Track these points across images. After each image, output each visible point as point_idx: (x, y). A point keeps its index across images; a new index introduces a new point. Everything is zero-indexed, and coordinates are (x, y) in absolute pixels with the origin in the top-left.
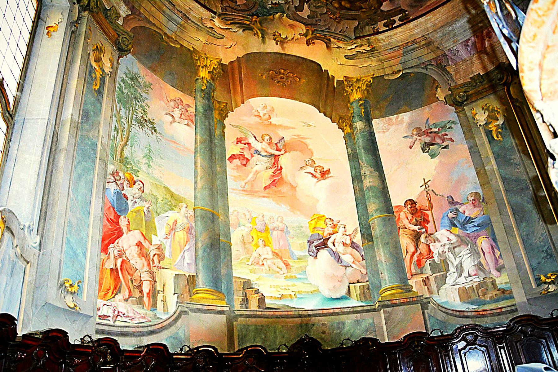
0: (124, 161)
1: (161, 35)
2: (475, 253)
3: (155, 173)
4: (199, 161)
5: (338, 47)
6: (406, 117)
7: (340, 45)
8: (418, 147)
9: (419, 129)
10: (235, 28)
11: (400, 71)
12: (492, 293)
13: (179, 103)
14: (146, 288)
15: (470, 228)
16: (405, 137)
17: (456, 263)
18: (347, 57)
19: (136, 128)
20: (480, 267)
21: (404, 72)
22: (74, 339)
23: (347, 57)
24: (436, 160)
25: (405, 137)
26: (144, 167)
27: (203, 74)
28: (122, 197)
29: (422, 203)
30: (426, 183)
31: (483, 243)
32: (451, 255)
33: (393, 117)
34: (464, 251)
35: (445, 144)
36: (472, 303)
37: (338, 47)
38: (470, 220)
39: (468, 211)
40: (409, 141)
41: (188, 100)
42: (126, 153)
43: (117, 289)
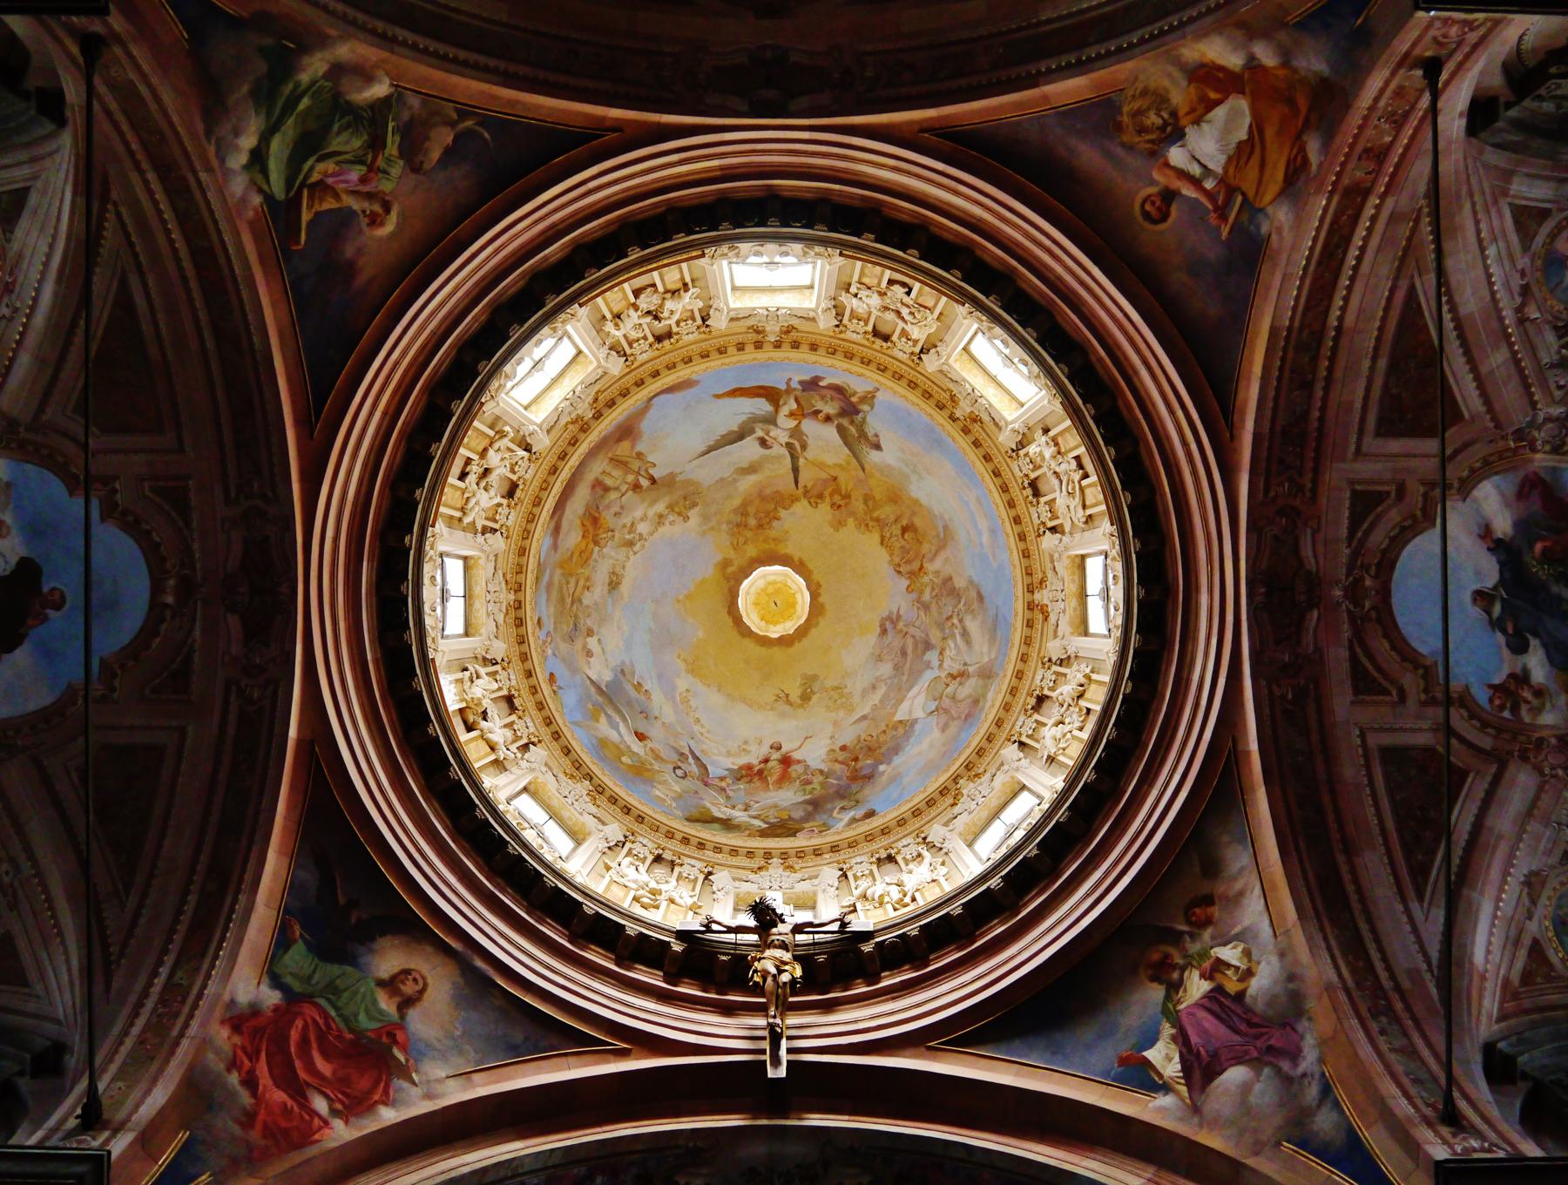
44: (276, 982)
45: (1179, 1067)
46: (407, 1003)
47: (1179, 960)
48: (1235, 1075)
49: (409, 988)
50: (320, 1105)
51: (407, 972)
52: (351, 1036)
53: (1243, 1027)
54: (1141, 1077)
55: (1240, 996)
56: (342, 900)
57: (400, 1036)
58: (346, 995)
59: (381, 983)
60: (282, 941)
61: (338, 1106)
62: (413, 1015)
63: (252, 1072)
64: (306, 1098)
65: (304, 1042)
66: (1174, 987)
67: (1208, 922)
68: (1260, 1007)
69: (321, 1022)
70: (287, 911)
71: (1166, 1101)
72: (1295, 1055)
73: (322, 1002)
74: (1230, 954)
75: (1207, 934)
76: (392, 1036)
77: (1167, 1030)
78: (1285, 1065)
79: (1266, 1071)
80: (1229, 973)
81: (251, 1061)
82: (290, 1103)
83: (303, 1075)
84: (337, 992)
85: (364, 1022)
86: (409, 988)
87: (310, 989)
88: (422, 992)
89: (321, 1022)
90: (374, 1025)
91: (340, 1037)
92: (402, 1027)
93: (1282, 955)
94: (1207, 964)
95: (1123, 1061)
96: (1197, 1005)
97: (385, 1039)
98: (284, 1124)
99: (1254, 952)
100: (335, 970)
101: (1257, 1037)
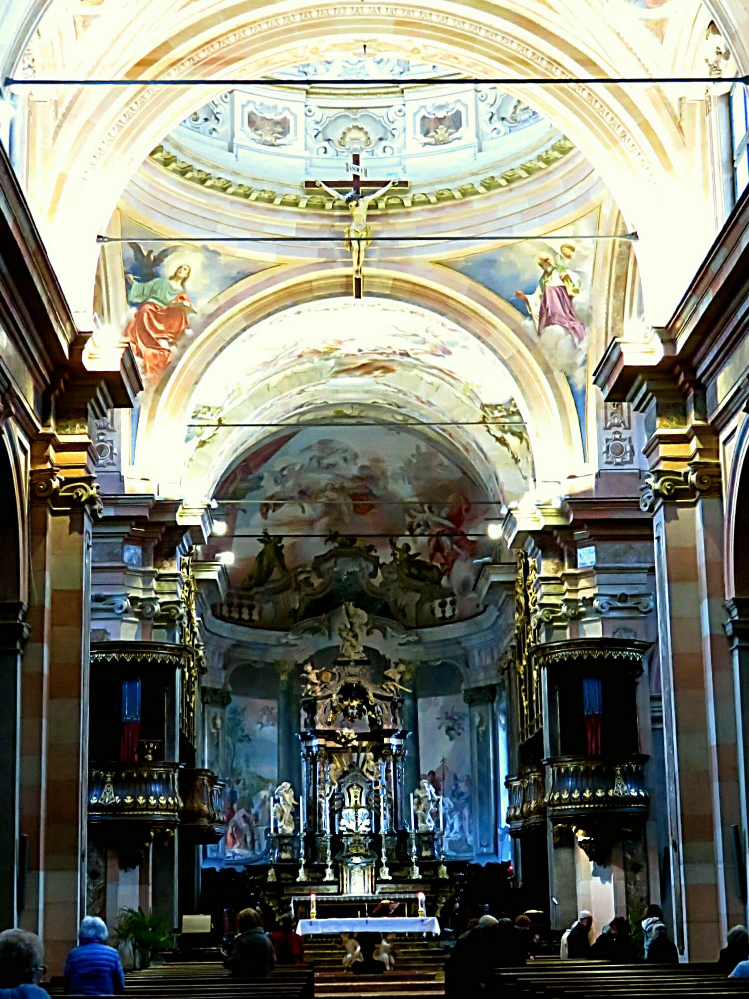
0: (233, 770)
1: (249, 665)
2: (461, 818)
3: (252, 769)
4: (281, 748)
5: (393, 636)
6: (441, 700)
7: (394, 634)
8: (443, 729)
9: (446, 713)
10: (306, 635)
11: (438, 660)
12: (464, 847)
13: (267, 710)
14: (249, 839)
15: (462, 801)
16: (438, 718)
17: (451, 822)
18: (400, 645)
19: (239, 745)
20: (461, 828)
21: (445, 661)
22: (218, 870)
23: (400, 645)
24: (452, 743)
25: (438, 718)
26: (244, 769)
27: (283, 677)
28: (233, 793)
29: (439, 775)
30: (443, 760)
31: (466, 812)
32: (449, 817)
33: (433, 698)
34: (456, 816)
35: (460, 731)
36: (454, 851)
37: (393, 636)
38: (462, 794)
39: (463, 787)
40: (439, 722)
41: (273, 704)
42: (234, 765)
43: (234, 843)
44: (132, 304)
45: (539, 310)
46: (185, 280)
47: (553, 265)
48: (556, 329)
49: (183, 274)
50: (164, 344)
51: (180, 267)
52: (165, 307)
53: (568, 311)
54: (521, 306)
55: (571, 298)
56: (145, 253)
57: (185, 296)
58: (159, 292)
59: (171, 278)
60: (128, 286)
61: (171, 340)
62: (187, 284)
63: (137, 347)
64: (158, 345)
65: (149, 319)
66: (547, 274)
67: (569, 257)
68: (577, 308)
69: (153, 309)
70: (126, 273)
71: (527, 323)
72: (580, 340)
73: (151, 300)
74: (574, 277)
75: (568, 261)
76: (182, 298)
77: (539, 291)
78: (576, 340)
79: (569, 336)
80: (571, 284)
81: (134, 343)
82: (155, 351)
83: (154, 336)
84: (155, 292)
85: (170, 298)
86: (183, 274)
87: (144, 298)
88: (189, 273)
89: (153, 309)
90: (173, 297)
91: (162, 311)
92: (185, 292)
93: (591, 296)
94: (563, 274)
95: (518, 295)
96: (554, 288)
97: (180, 301)
98: (156, 362)
99: (582, 284)
100: (151, 283)
101: (572, 320)
